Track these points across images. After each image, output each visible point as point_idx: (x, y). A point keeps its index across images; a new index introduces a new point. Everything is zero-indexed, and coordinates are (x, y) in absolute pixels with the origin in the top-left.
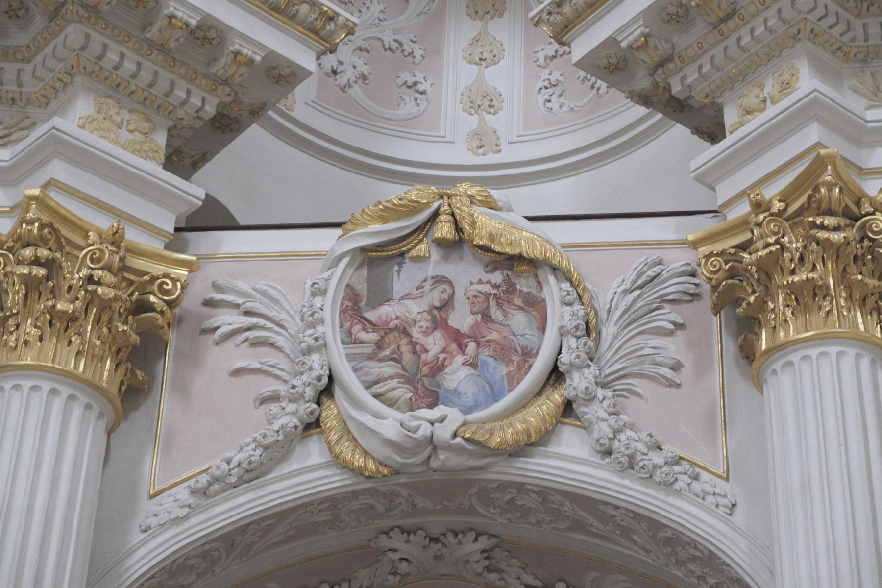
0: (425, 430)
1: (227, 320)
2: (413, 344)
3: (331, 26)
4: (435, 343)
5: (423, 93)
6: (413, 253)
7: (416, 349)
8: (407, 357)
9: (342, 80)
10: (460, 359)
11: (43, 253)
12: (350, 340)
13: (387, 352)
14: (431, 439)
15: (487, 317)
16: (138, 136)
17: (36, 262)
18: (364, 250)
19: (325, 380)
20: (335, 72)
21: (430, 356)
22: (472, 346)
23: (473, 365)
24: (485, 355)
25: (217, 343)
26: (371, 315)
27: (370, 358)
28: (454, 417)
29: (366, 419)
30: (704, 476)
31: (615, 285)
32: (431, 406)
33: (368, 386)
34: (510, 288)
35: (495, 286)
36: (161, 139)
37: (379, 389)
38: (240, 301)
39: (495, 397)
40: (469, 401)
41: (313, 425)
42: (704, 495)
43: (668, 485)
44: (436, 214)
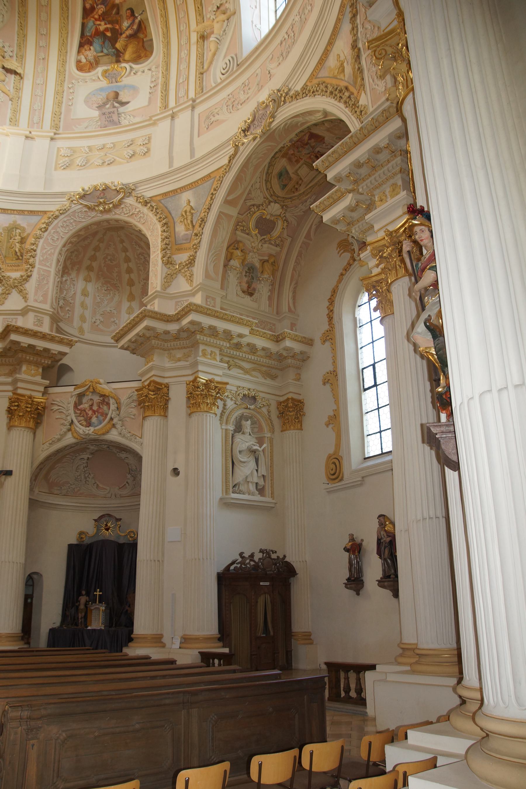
0: (87, 432)
1: (55, 408)
2: (86, 413)
3: (72, 342)
4: (90, 413)
5: (116, 323)
6: (86, 394)
7: (87, 414)
8: (85, 416)
9: (97, 324)
10: (94, 416)
11: (16, 404)
12: (75, 413)
13: (82, 415)
14: (88, 433)
15: (99, 407)
16: (36, 371)
17: (15, 406)
18: (77, 394)
19: (71, 421)
20: (95, 322)
21: (89, 416)
22: (97, 413)
23: (97, 417)
24: (99, 415)
25: (53, 412)
26: (79, 407)
27: (78, 416)
28: (92, 429)
29: (78, 429)
30: (138, 438)
31: (125, 398)
32: (88, 427)
33: (79, 422)
34: (104, 400)
35: (101, 400)
36: (40, 370)
37: (80, 422)
38: (57, 403)
39: (100, 423)
40: (96, 425)
41: (69, 430)
42: (137, 442)
43: (131, 440)
44: (90, 386)
